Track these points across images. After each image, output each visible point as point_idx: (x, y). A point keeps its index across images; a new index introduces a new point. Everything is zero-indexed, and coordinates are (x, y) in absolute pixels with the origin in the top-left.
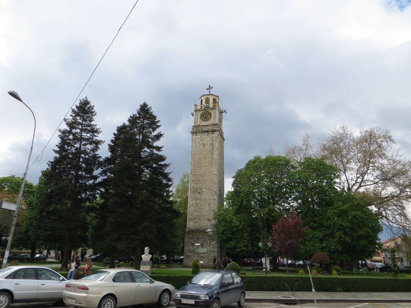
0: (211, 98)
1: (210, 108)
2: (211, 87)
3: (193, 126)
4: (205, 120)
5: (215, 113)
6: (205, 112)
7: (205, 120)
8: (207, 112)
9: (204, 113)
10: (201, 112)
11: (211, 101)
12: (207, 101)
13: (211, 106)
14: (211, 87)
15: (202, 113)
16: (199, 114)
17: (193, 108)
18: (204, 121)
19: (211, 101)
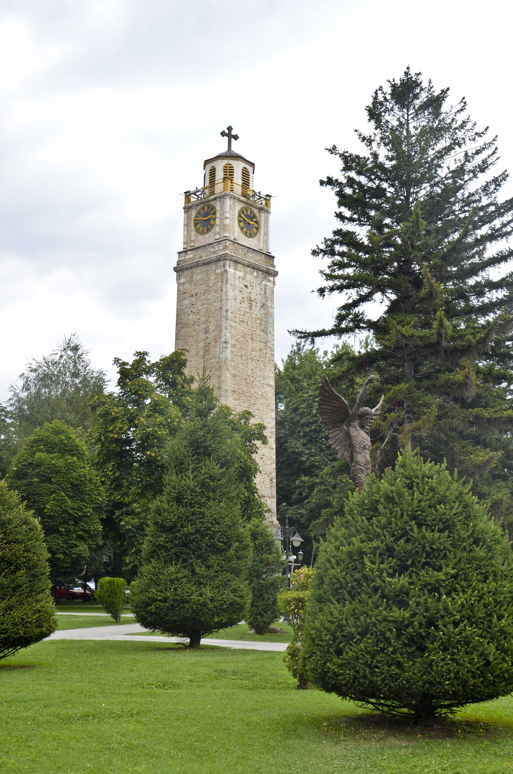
0: (220, 166)
1: (213, 197)
2: (227, 131)
3: (181, 250)
4: (203, 229)
5: (222, 206)
6: (203, 209)
7: (203, 229)
8: (208, 207)
9: (202, 212)
10: (199, 207)
11: (220, 175)
12: (213, 172)
13: (219, 188)
14: (227, 131)
15: (199, 213)
16: (194, 213)
17: (181, 201)
18: (203, 233)
19: (220, 175)
